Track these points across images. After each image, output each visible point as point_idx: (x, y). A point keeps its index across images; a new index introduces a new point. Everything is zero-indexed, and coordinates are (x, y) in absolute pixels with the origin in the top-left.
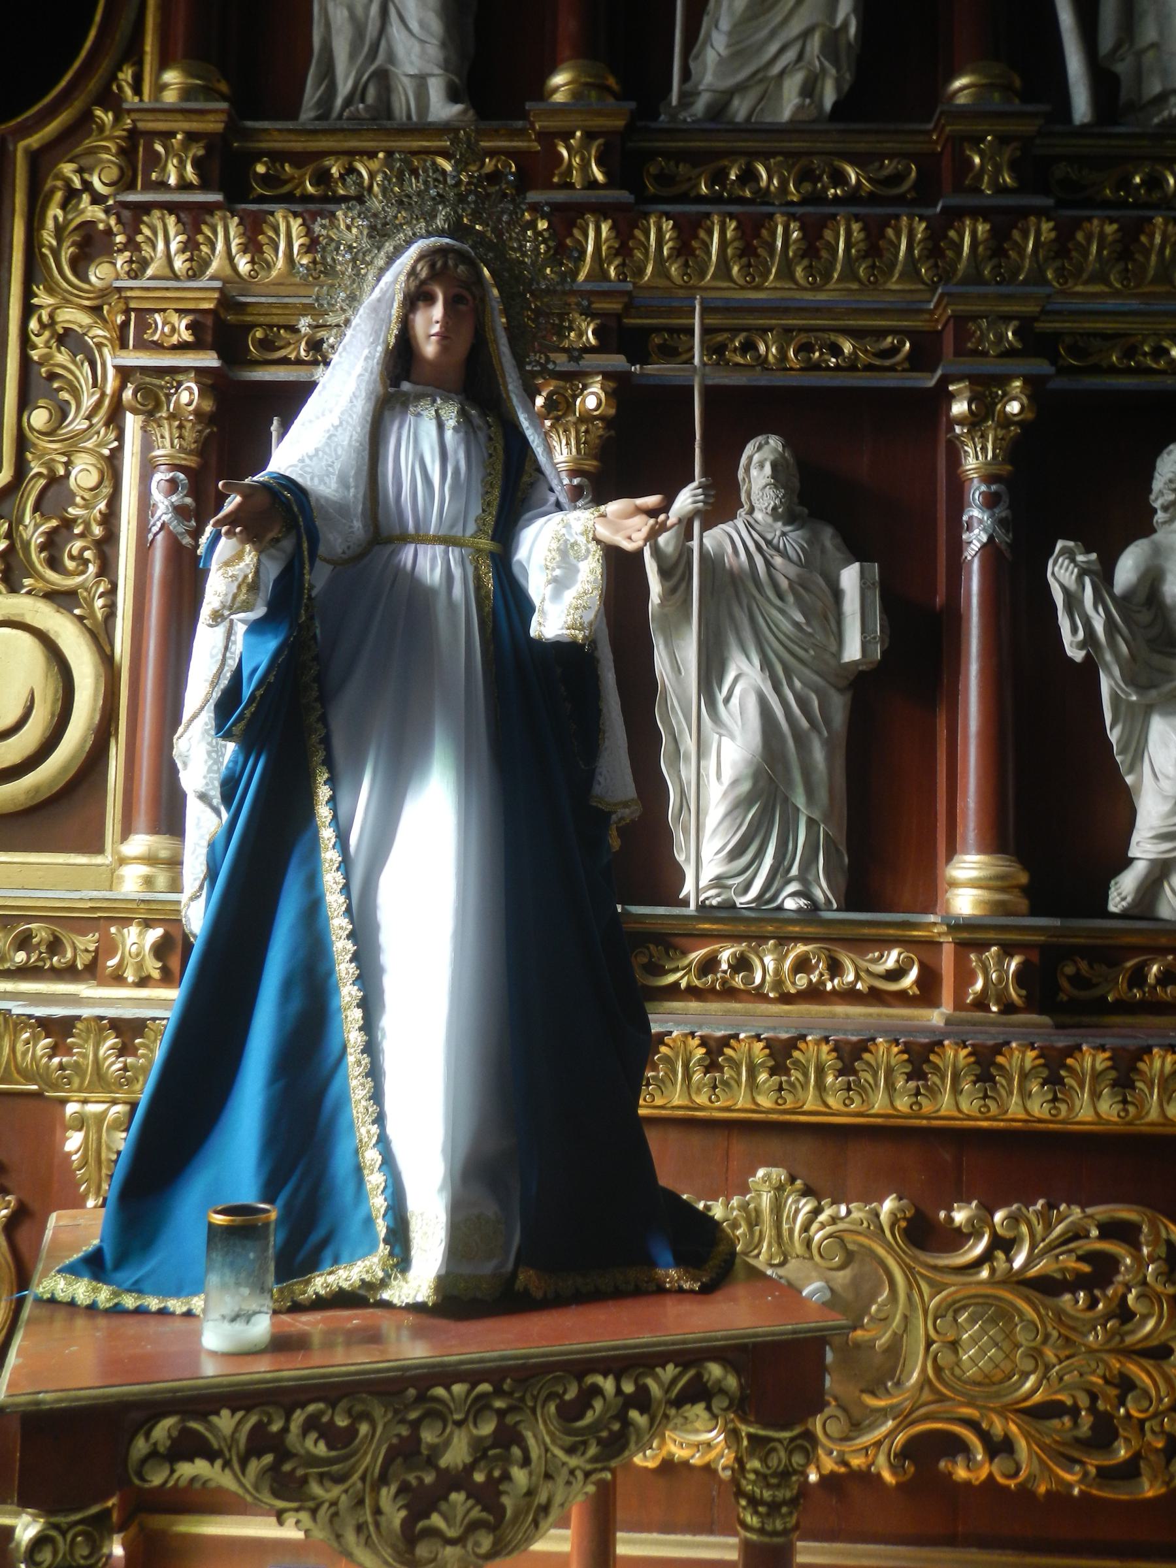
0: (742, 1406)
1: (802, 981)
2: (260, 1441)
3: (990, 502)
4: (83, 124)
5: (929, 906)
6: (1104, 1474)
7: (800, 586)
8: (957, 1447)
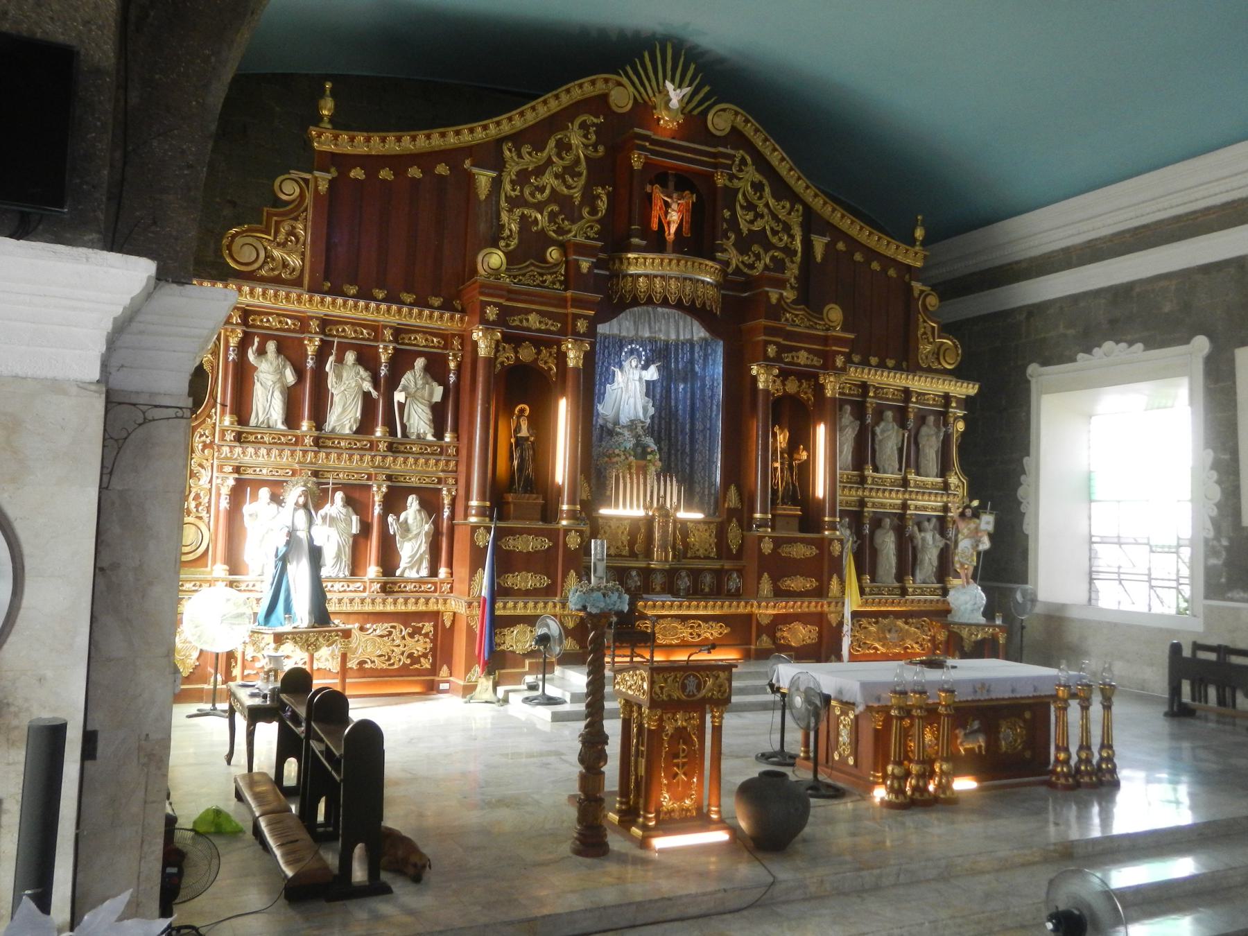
0: (342, 637)
1: (343, 589)
2: (294, 638)
3: (380, 505)
4: (204, 422)
5: (365, 576)
6: (390, 665)
7: (345, 520)
8: (366, 662)
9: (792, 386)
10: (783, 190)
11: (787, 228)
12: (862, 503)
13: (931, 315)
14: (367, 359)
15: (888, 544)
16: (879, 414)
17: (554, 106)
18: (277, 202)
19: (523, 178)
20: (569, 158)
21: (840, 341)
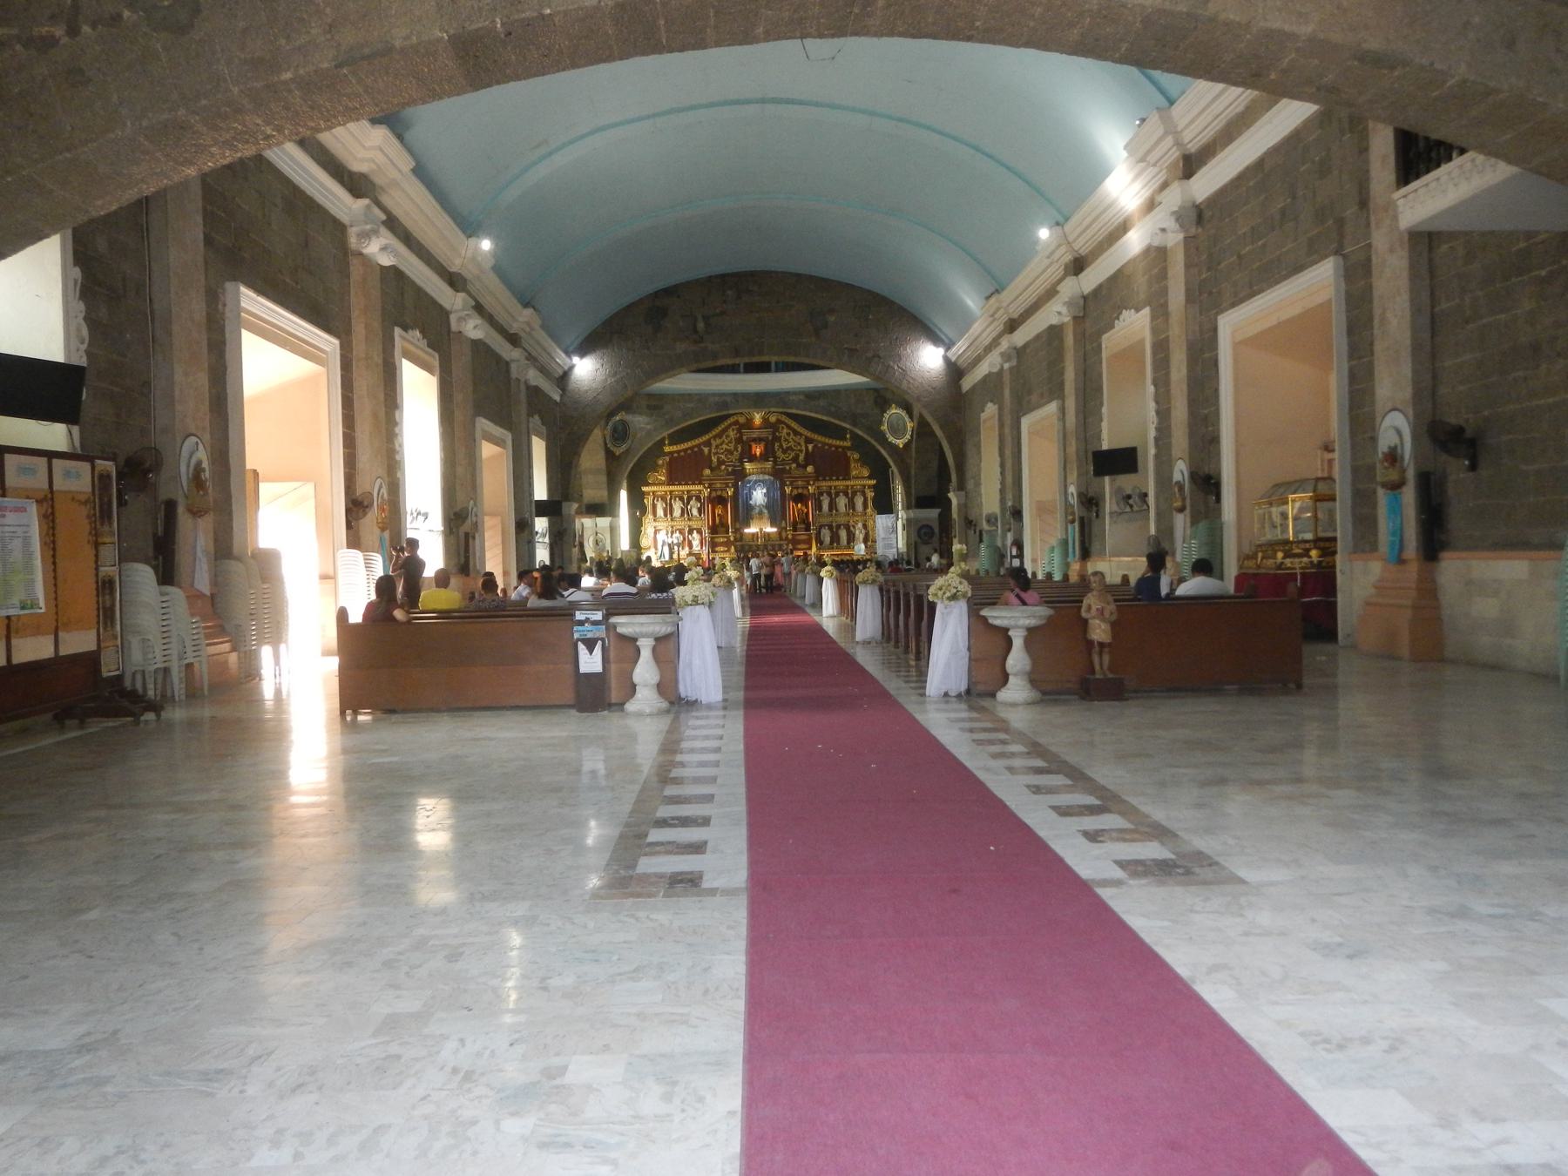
9: (800, 491)
10: (796, 433)
11: (799, 444)
12: (832, 522)
13: (856, 461)
14: (681, 499)
15: (843, 534)
16: (837, 495)
17: (723, 426)
18: (658, 465)
19: (717, 447)
20: (729, 439)
21: (811, 477)
